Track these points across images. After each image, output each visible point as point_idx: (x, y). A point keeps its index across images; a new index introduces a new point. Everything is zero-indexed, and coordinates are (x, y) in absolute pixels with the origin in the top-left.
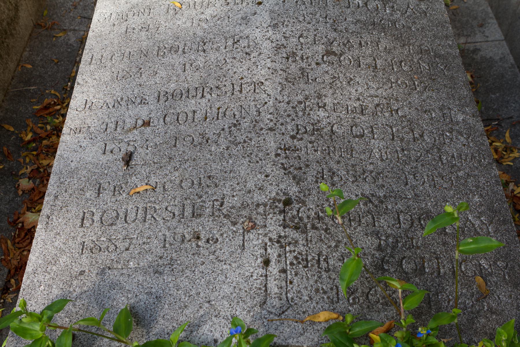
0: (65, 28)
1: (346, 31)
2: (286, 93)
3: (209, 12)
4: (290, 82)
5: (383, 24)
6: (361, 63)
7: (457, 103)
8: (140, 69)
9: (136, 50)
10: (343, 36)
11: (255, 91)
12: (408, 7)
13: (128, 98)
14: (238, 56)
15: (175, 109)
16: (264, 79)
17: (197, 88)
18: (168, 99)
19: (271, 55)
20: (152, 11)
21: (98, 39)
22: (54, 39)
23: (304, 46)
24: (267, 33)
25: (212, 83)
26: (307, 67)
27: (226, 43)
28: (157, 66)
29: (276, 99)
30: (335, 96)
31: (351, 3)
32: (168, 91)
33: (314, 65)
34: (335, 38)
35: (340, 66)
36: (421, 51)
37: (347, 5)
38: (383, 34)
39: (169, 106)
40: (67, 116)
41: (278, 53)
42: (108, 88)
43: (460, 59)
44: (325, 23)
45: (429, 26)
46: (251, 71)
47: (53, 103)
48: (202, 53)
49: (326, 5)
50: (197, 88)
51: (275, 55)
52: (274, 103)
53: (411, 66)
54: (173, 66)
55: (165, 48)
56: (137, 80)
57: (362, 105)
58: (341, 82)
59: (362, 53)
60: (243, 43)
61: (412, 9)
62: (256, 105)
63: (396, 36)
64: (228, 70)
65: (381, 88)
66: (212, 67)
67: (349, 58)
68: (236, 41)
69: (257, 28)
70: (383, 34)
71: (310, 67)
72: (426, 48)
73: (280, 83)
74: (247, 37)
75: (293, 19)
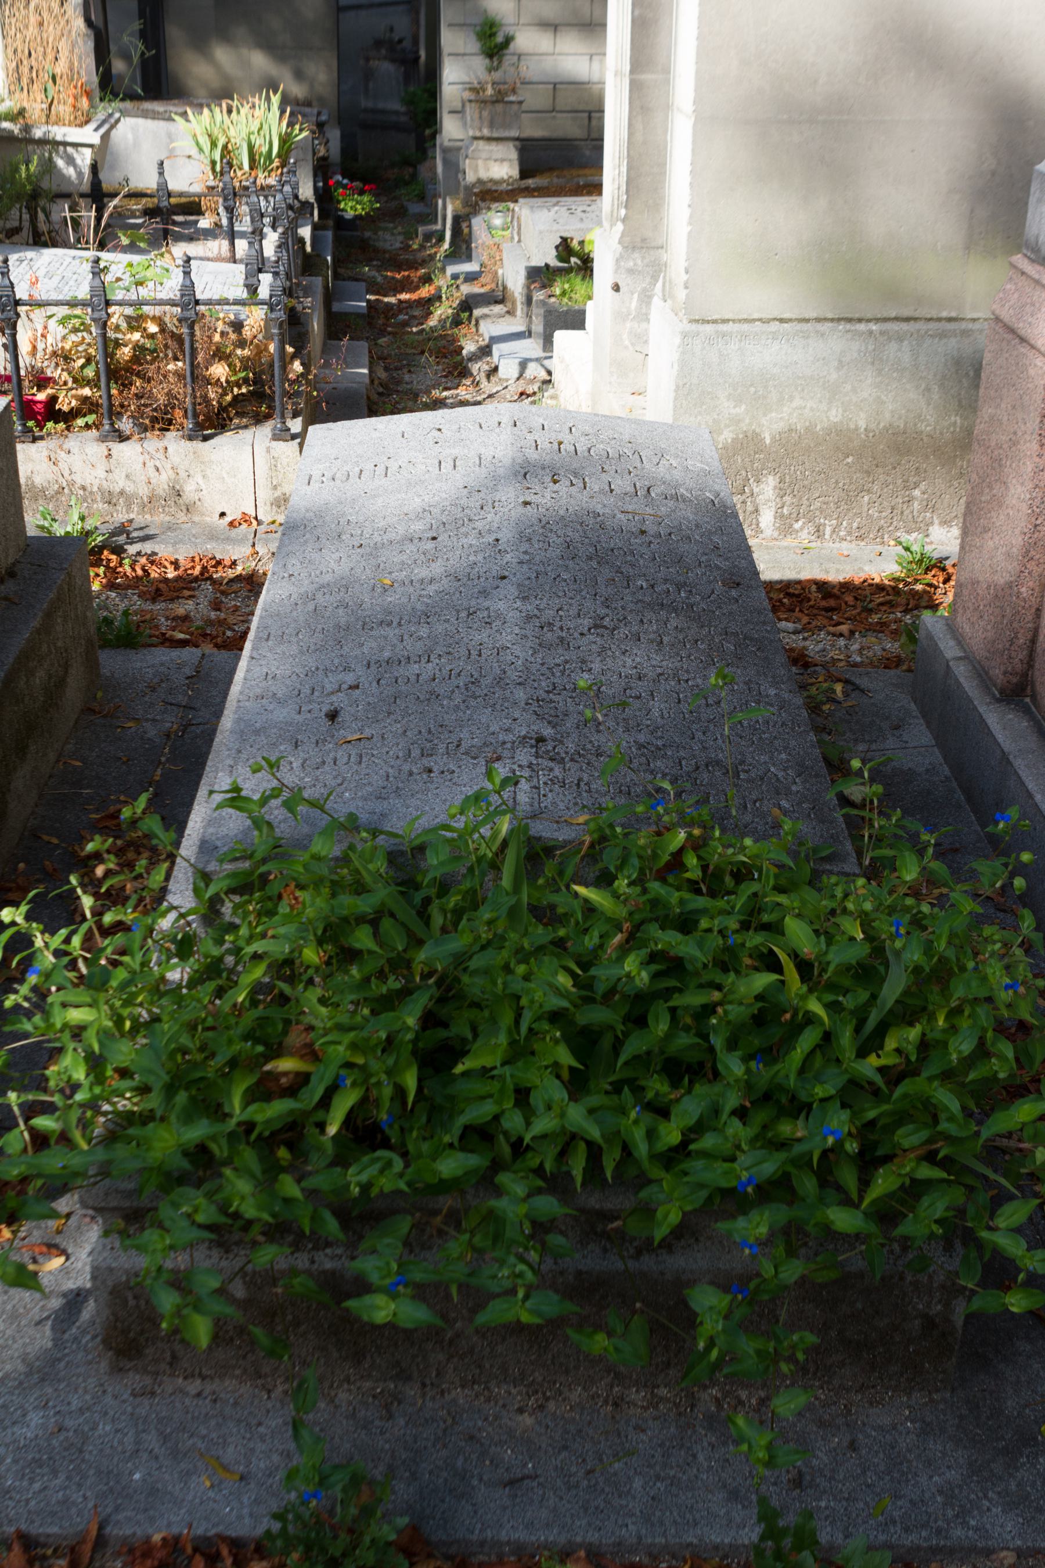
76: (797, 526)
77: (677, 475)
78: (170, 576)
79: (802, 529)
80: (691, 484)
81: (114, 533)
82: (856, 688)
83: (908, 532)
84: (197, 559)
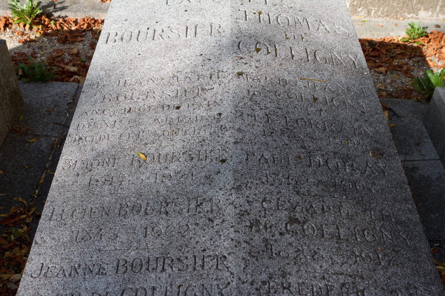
0: (38, 133)
1: (309, 194)
2: (250, 271)
3: (173, 167)
4: (253, 257)
5: (344, 185)
6: (325, 232)
7: (423, 280)
8: (101, 230)
9: (97, 206)
10: (306, 200)
11: (217, 267)
12: (367, 165)
13: (86, 265)
14: (201, 222)
15: (134, 283)
16: (227, 252)
17: (157, 258)
18: (127, 269)
19: (234, 224)
20: (116, 161)
21: (61, 190)
22: (27, 145)
23: (267, 213)
24: (230, 197)
25: (173, 253)
26: (271, 237)
27: (189, 205)
28: (118, 228)
29: (240, 279)
30: (300, 273)
31: (312, 161)
32: (128, 260)
33: (277, 236)
34: (298, 203)
35: (304, 236)
36: (383, 217)
37: (308, 163)
38: (344, 197)
39: (128, 279)
40: (21, 283)
41: (242, 221)
42: (67, 251)
43: (421, 226)
44: (288, 184)
45: (388, 187)
46: (214, 242)
47: (19, 211)
48: (164, 216)
49: (288, 163)
50: (157, 258)
51: (238, 224)
52: (237, 284)
53: (373, 236)
54: (134, 229)
55: (127, 206)
56: (96, 243)
57: (327, 285)
58: (305, 256)
59: (325, 220)
60: (206, 207)
61: (371, 168)
62: (218, 285)
63: (357, 200)
64: (191, 239)
65: (346, 263)
66: (174, 233)
67: (312, 226)
68: (199, 204)
69: (220, 189)
70: (344, 197)
71: (274, 238)
72: (387, 213)
73: (243, 259)
74: (211, 199)
75: (256, 179)
76: (359, 10)
77: (331, 38)
78: (73, 28)
79: (361, 11)
80: (339, 47)
81: (48, 6)
82: (395, 114)
83: (409, 14)
84: (86, 20)
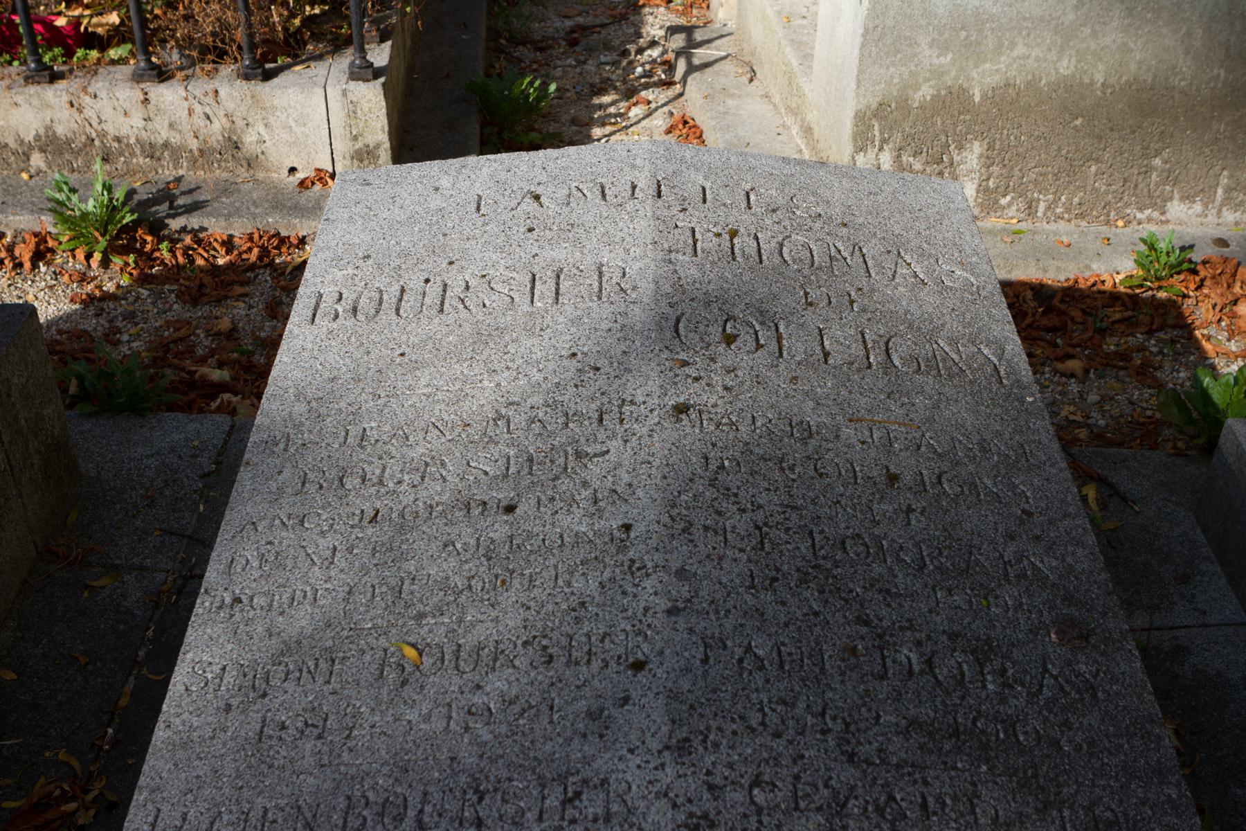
0: (118, 562)
1: (883, 761)
3: (497, 683)
5: (983, 732)
9: (283, 802)
10: (875, 779)
12: (1046, 670)
21: (181, 754)
22: (86, 594)
23: (765, 820)
24: (660, 774)
27: (544, 798)
31: (889, 662)
34: (853, 788)
36: (1096, 825)
38: (984, 768)
44: (823, 732)
45: (1107, 736)
47: (57, 792)
49: (822, 669)
55: (367, 804)
61: (1055, 678)
63: (1021, 775)
69: (631, 751)
70: (984, 768)
72: (1108, 814)
74: (605, 782)
75: (733, 720)
76: (1004, 201)
77: (929, 298)
78: (221, 262)
79: (1009, 205)
80: (953, 326)
81: (155, 201)
82: (1115, 492)
83: (1141, 210)
84: (256, 236)
